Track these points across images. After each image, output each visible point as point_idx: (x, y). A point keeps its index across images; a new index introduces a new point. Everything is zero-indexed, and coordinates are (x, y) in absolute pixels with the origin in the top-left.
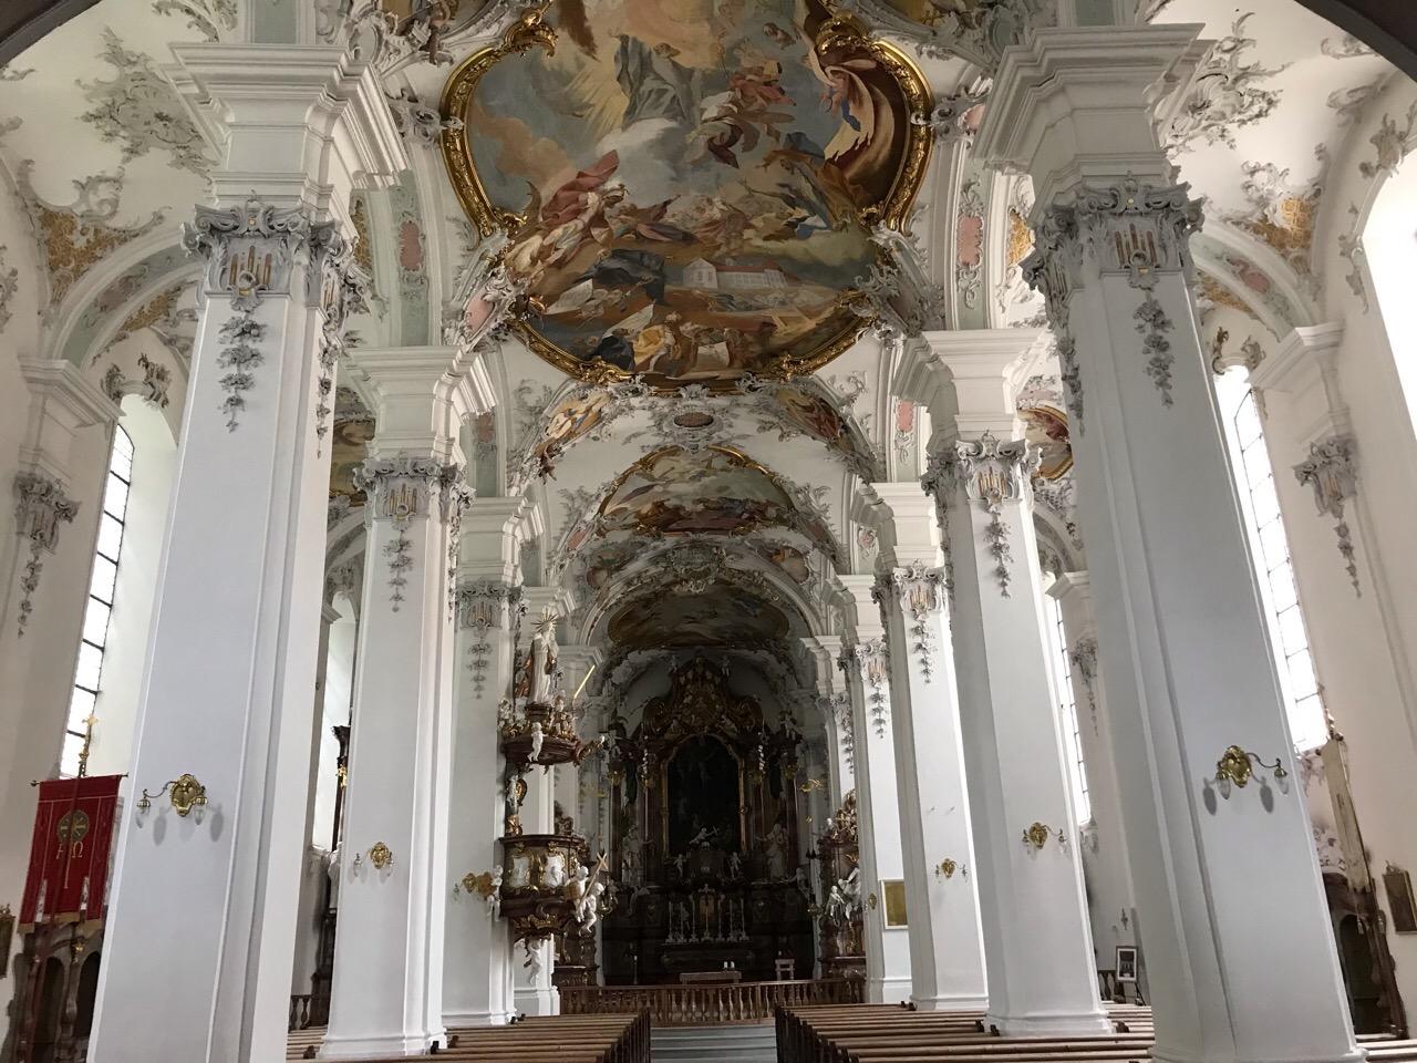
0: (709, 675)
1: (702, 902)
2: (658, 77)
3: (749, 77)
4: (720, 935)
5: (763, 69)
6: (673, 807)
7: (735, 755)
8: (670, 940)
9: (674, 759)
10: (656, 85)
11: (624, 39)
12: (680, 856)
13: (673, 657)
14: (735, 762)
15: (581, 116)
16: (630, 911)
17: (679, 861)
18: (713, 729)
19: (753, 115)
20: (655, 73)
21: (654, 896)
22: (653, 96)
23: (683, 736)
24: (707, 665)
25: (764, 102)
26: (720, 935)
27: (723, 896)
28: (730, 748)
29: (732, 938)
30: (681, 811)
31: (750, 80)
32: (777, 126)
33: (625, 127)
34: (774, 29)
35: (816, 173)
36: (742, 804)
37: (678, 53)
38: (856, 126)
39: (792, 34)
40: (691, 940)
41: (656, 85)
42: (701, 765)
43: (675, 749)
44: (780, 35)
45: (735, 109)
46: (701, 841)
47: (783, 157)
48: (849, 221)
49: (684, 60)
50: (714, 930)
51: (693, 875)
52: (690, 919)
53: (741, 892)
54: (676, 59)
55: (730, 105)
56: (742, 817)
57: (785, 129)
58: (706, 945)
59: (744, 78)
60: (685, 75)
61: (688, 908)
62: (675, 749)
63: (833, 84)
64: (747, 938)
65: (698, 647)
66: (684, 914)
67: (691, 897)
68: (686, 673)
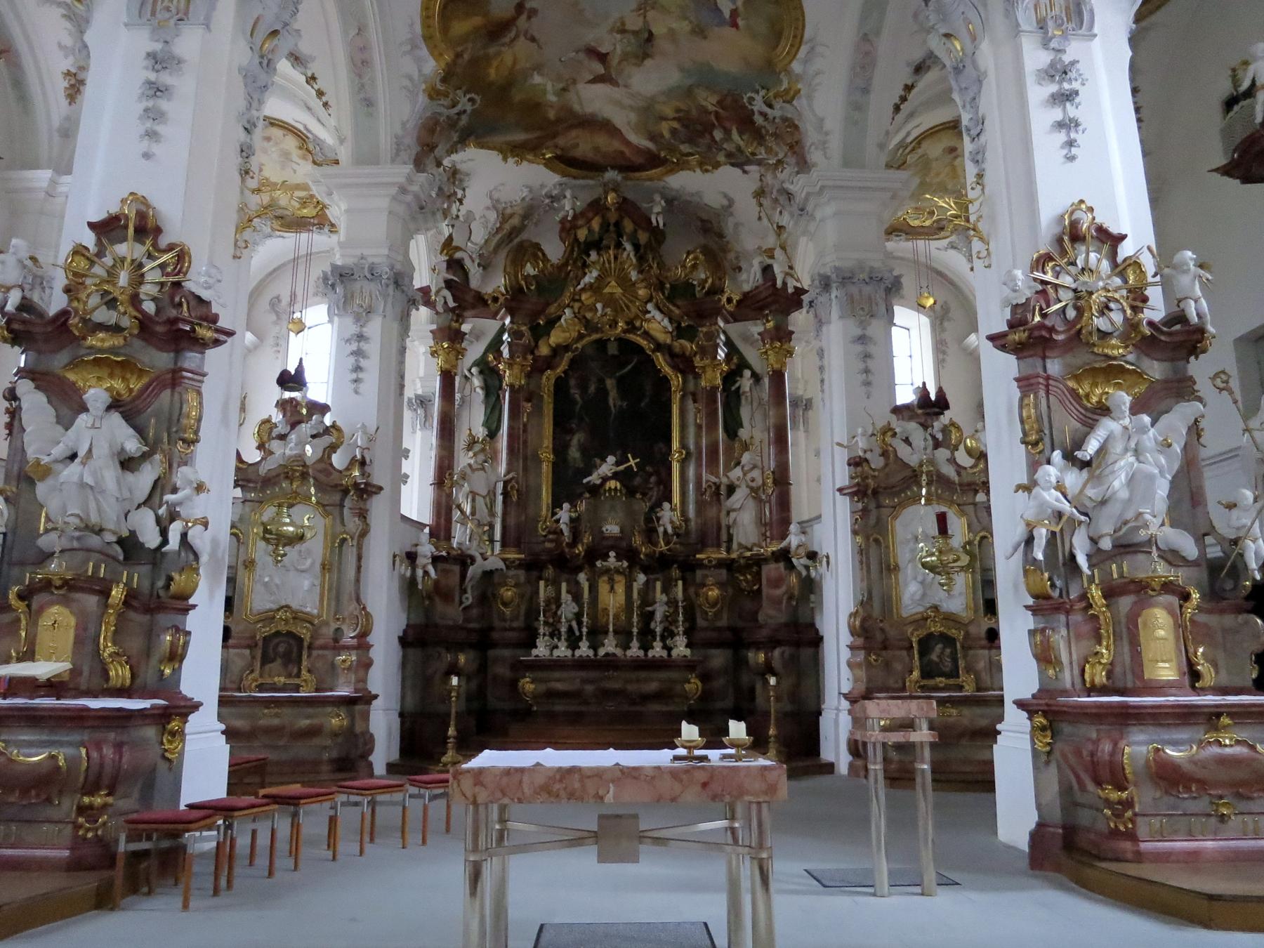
0: (628, 226)
1: (603, 587)
4: (635, 644)
6: (560, 450)
7: (667, 370)
8: (541, 650)
9: (565, 372)
12: (566, 506)
13: (568, 194)
14: (666, 380)
16: (469, 598)
17: (564, 514)
18: (631, 327)
21: (512, 572)
23: (581, 337)
24: (625, 206)
26: (635, 644)
27: (642, 578)
28: (661, 360)
29: (657, 651)
30: (574, 453)
36: (675, 445)
40: (578, 653)
42: (610, 383)
43: (569, 355)
46: (605, 479)
50: (624, 636)
51: (587, 539)
52: (578, 616)
53: (675, 573)
56: (676, 467)
58: (610, 663)
61: (577, 598)
62: (569, 355)
64: (688, 652)
65: (611, 175)
66: (568, 608)
67: (582, 577)
68: (589, 221)
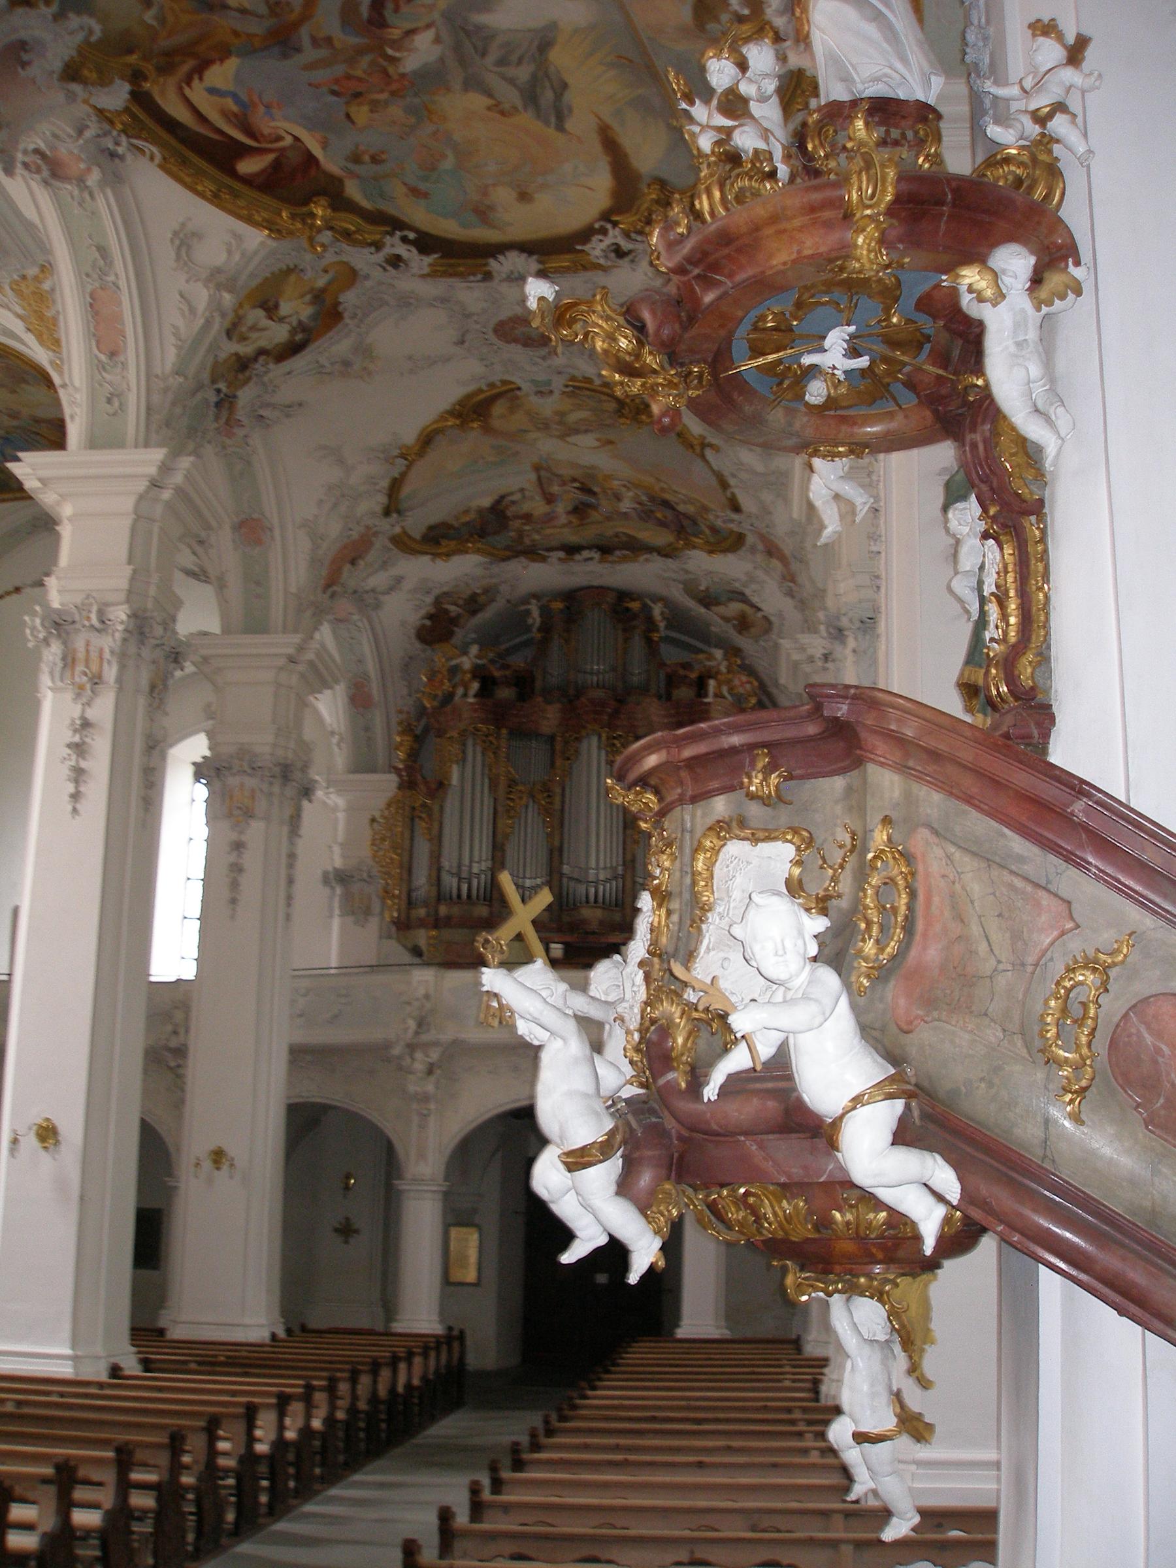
2: (512, 81)
3: (384, 96)
5: (372, 111)
10: (511, 72)
11: (560, 128)
15: (620, 57)
19: (360, 51)
20: (515, 85)
22: (514, 58)
25: (352, 72)
31: (382, 91)
32: (323, 53)
33: (553, 26)
34: (375, 160)
35: (236, 34)
37: (489, 108)
38: (212, 91)
39: (350, 166)
41: (511, 72)
44: (367, 158)
45: (390, 52)
47: (294, 16)
48: (149, 17)
49: (477, 101)
54: (490, 102)
55: (397, 55)
57: (310, 54)
59: (393, 93)
60: (473, 83)
63: (273, 124)
